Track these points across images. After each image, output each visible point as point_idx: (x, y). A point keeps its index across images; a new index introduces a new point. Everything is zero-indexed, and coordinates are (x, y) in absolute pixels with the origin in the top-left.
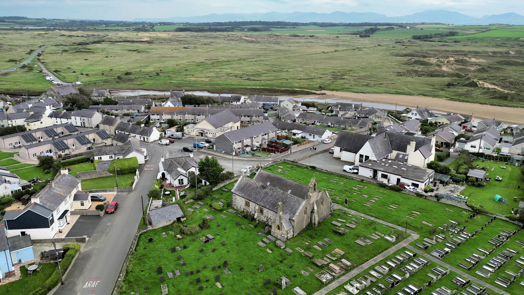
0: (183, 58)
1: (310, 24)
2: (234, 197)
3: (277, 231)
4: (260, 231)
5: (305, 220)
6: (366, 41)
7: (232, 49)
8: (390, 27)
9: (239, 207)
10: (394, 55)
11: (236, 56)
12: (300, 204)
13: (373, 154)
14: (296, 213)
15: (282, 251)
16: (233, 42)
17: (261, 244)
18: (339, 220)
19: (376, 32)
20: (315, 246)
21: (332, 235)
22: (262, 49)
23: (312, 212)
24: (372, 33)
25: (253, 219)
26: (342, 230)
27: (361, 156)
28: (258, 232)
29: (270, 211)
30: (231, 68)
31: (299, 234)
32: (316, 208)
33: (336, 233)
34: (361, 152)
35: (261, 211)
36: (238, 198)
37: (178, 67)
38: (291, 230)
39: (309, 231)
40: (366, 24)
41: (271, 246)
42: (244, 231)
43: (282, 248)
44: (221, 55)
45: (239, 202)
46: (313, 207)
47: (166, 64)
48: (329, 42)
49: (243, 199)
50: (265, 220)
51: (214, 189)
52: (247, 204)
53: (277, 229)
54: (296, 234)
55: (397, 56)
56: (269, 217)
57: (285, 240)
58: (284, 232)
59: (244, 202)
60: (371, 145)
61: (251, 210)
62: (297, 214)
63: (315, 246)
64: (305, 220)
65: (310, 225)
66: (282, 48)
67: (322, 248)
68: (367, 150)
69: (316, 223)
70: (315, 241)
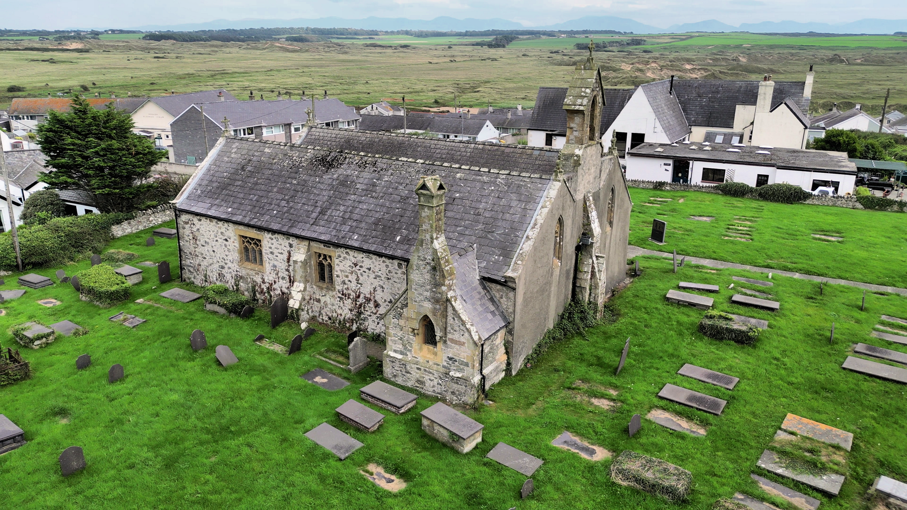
0: (150, 70)
1: (398, 33)
2: (186, 232)
3: (421, 353)
4: (321, 370)
5: (554, 289)
6: (500, 52)
7: (255, 59)
8: (534, 34)
9: (213, 276)
10: (556, 65)
11: (263, 67)
12: (530, 200)
13: (658, 124)
14: (515, 243)
15: (472, 470)
16: (258, 52)
17: (329, 438)
18: (682, 284)
19: (514, 42)
20: (659, 416)
21: (703, 346)
22: (314, 60)
23: (583, 247)
24: (508, 44)
25: (281, 314)
26: (738, 323)
27: (620, 137)
28: (308, 374)
29: (368, 262)
30: (251, 81)
31: (537, 359)
32: (596, 227)
33: (716, 334)
34: (618, 125)
35: (324, 272)
36: (206, 228)
37: (133, 81)
38: (499, 340)
39: (577, 340)
40: (493, 33)
41: (396, 441)
42: (227, 376)
43: (468, 447)
44: (230, 66)
45: (215, 250)
46: (587, 224)
47: (108, 77)
48: (436, 53)
49: (232, 232)
50: (345, 311)
51: (117, 231)
52: (251, 251)
53: (416, 342)
54: (518, 364)
55: (560, 65)
56: (366, 290)
57: (470, 397)
58: (466, 353)
59: (235, 244)
60: (648, 97)
61: (269, 277)
62: (526, 246)
63: (659, 416)
64: (554, 289)
65: (575, 316)
66: (352, 58)
67: (704, 423)
68: (639, 115)
69: (601, 300)
70: (639, 389)
